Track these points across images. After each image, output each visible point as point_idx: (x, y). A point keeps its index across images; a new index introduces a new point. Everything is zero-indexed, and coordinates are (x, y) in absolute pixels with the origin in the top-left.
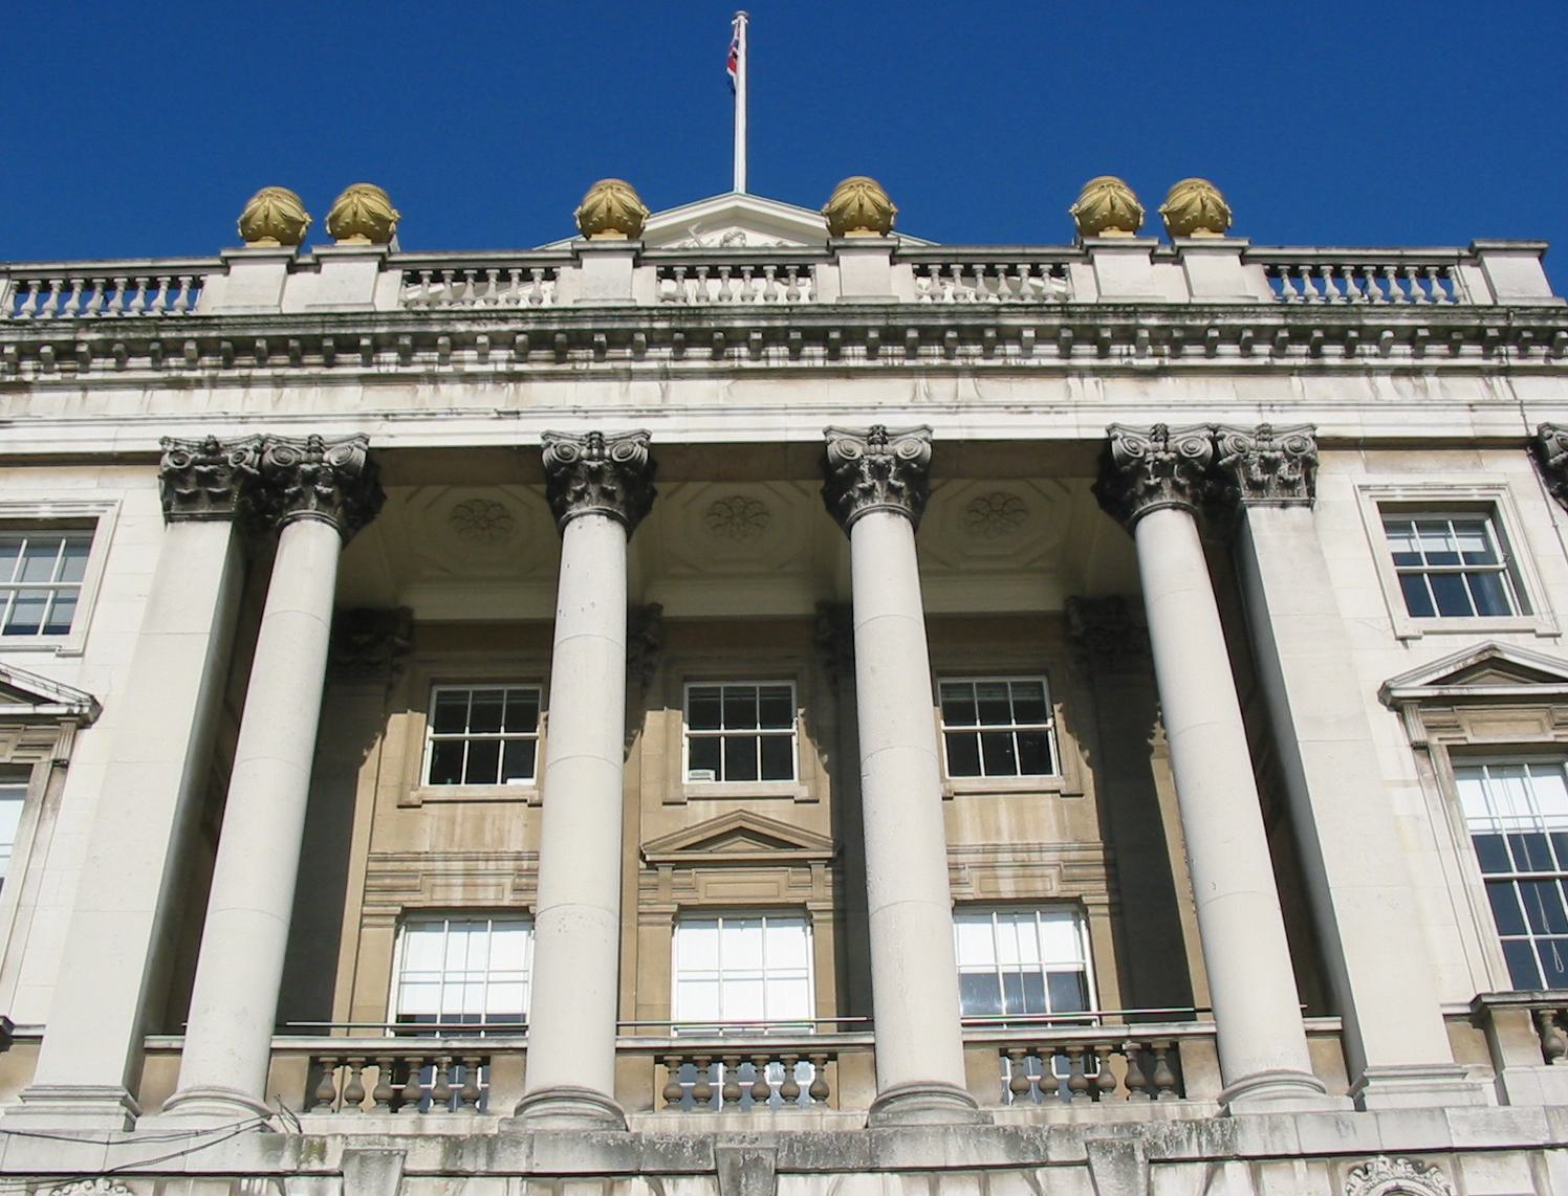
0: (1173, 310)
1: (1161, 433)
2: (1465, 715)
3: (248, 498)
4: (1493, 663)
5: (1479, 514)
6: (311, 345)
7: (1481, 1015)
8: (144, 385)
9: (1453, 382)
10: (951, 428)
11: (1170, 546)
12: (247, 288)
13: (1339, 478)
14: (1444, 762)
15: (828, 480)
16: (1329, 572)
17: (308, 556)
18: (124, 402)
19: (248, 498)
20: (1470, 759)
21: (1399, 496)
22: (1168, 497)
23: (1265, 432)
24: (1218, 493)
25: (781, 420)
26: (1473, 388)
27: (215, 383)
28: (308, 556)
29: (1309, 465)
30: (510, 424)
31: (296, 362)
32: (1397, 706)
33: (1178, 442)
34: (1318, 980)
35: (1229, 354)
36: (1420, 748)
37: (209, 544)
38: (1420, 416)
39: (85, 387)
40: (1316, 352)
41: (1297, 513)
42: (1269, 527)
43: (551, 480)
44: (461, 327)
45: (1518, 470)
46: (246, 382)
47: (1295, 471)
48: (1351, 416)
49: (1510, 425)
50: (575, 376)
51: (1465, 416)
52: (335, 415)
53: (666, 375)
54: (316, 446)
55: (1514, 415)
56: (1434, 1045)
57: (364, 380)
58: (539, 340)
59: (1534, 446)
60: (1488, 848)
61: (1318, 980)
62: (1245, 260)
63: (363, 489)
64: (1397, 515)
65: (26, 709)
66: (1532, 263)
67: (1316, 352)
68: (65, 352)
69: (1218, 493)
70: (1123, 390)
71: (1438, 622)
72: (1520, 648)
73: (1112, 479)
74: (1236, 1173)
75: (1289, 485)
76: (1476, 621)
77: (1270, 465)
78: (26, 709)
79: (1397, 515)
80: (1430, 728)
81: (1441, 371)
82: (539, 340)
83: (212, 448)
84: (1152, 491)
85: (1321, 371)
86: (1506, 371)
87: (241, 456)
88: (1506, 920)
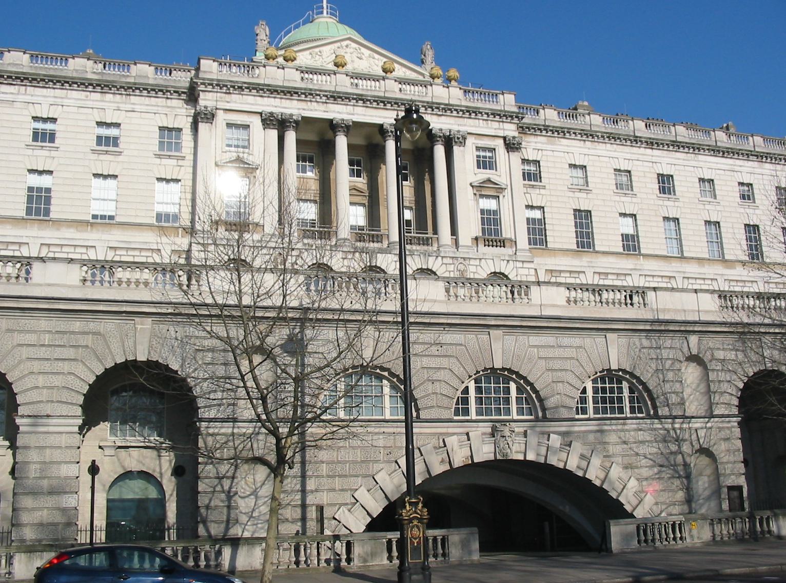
0: (446, 105)
1: (441, 130)
2: (483, 189)
5: (493, 150)
6: (289, 92)
7: (476, 239)
8: (254, 96)
9: (493, 123)
11: (439, 151)
12: (271, 75)
13: (470, 141)
14: (478, 196)
16: (465, 157)
17: (291, 137)
18: (250, 99)
20: (482, 196)
21: (479, 145)
23: (459, 131)
24: (449, 142)
25: (375, 118)
27: (269, 97)
28: (291, 137)
29: (465, 139)
30: (326, 113)
31: (285, 95)
32: (473, 186)
33: (443, 131)
34: (454, 231)
36: (475, 194)
37: (273, 134)
38: (485, 130)
39: (242, 95)
40: (470, 114)
41: (462, 148)
42: (456, 149)
44: (318, 93)
45: (501, 141)
46: (275, 98)
47: (462, 141)
48: (474, 129)
49: (501, 133)
50: (337, 104)
51: (494, 131)
52: (293, 108)
53: (354, 105)
54: (291, 115)
55: (502, 131)
57: (298, 100)
59: (505, 138)
60: (482, 212)
61: (454, 231)
62: (460, 89)
64: (478, 149)
66: (513, 96)
67: (470, 114)
68: (240, 88)
69: (449, 142)
71: (482, 170)
72: (494, 178)
74: (440, 258)
75: (461, 142)
76: (488, 171)
77: (458, 138)
79: (478, 149)
80: (477, 191)
81: (492, 121)
82: (332, 96)
83: (272, 114)
84: (438, 141)
85: (470, 118)
86: (503, 122)
87: (278, 115)
88: (483, 224)
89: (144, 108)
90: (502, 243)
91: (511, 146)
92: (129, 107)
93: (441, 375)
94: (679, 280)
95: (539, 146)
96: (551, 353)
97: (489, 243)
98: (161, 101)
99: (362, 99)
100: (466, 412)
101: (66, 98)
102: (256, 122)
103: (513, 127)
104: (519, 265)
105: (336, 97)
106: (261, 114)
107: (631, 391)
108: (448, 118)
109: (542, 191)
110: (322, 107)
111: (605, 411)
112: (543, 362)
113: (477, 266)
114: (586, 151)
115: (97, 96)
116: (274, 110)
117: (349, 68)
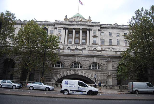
3: (65, 29)
4: (95, 35)
10: (83, 28)
11: (88, 32)
15: (80, 29)
16: (92, 33)
19: (65, 29)
24: (89, 30)
26: (97, 27)
28: (67, 31)
37: (64, 30)
43: (73, 29)
47: (91, 30)
58: (72, 25)
63: (68, 29)
69: (89, 30)
70: (88, 27)
73: (87, 29)
90: (96, 44)
91: (99, 30)
93: (68, 62)
94: (111, 49)
95: (104, 30)
96: (85, 60)
97: (94, 44)
98: (51, 27)
99: (77, 25)
100: (72, 67)
102: (62, 29)
103: (100, 27)
105: (73, 25)
107: (99, 66)
110: (71, 26)
111: (94, 68)
112: (84, 61)
116: (65, 27)
117: (76, 20)
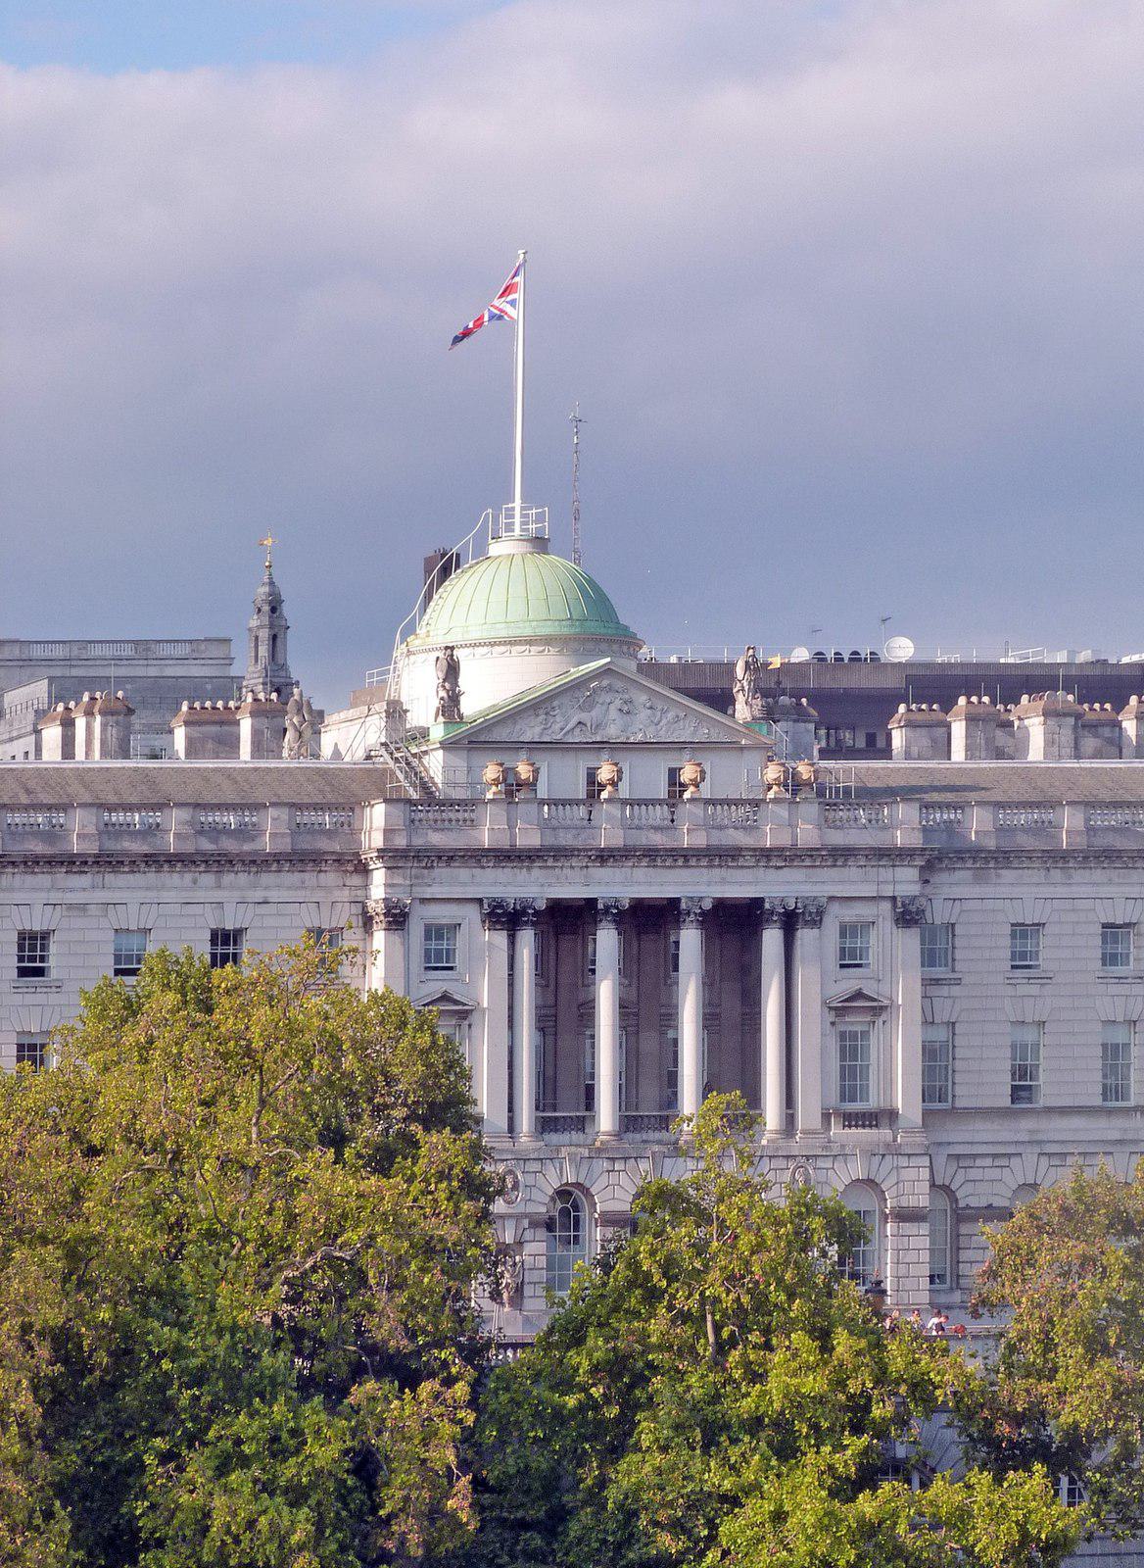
3: (506, 918)
11: (771, 939)
22: (778, 925)
24: (790, 922)
28: (527, 938)
35: (808, 863)
41: (816, 931)
42: (805, 936)
56: (816, 1123)
65: (460, 1007)
78: (460, 1007)
85: (835, 866)
89: (285, 895)
90: (870, 1119)
92: (259, 895)
101: (163, 887)
102: (472, 915)
104: (903, 1161)
106: (480, 901)
108: (795, 870)
109: (956, 990)
113: (827, 1169)
114: (1047, 891)
115: (208, 879)
